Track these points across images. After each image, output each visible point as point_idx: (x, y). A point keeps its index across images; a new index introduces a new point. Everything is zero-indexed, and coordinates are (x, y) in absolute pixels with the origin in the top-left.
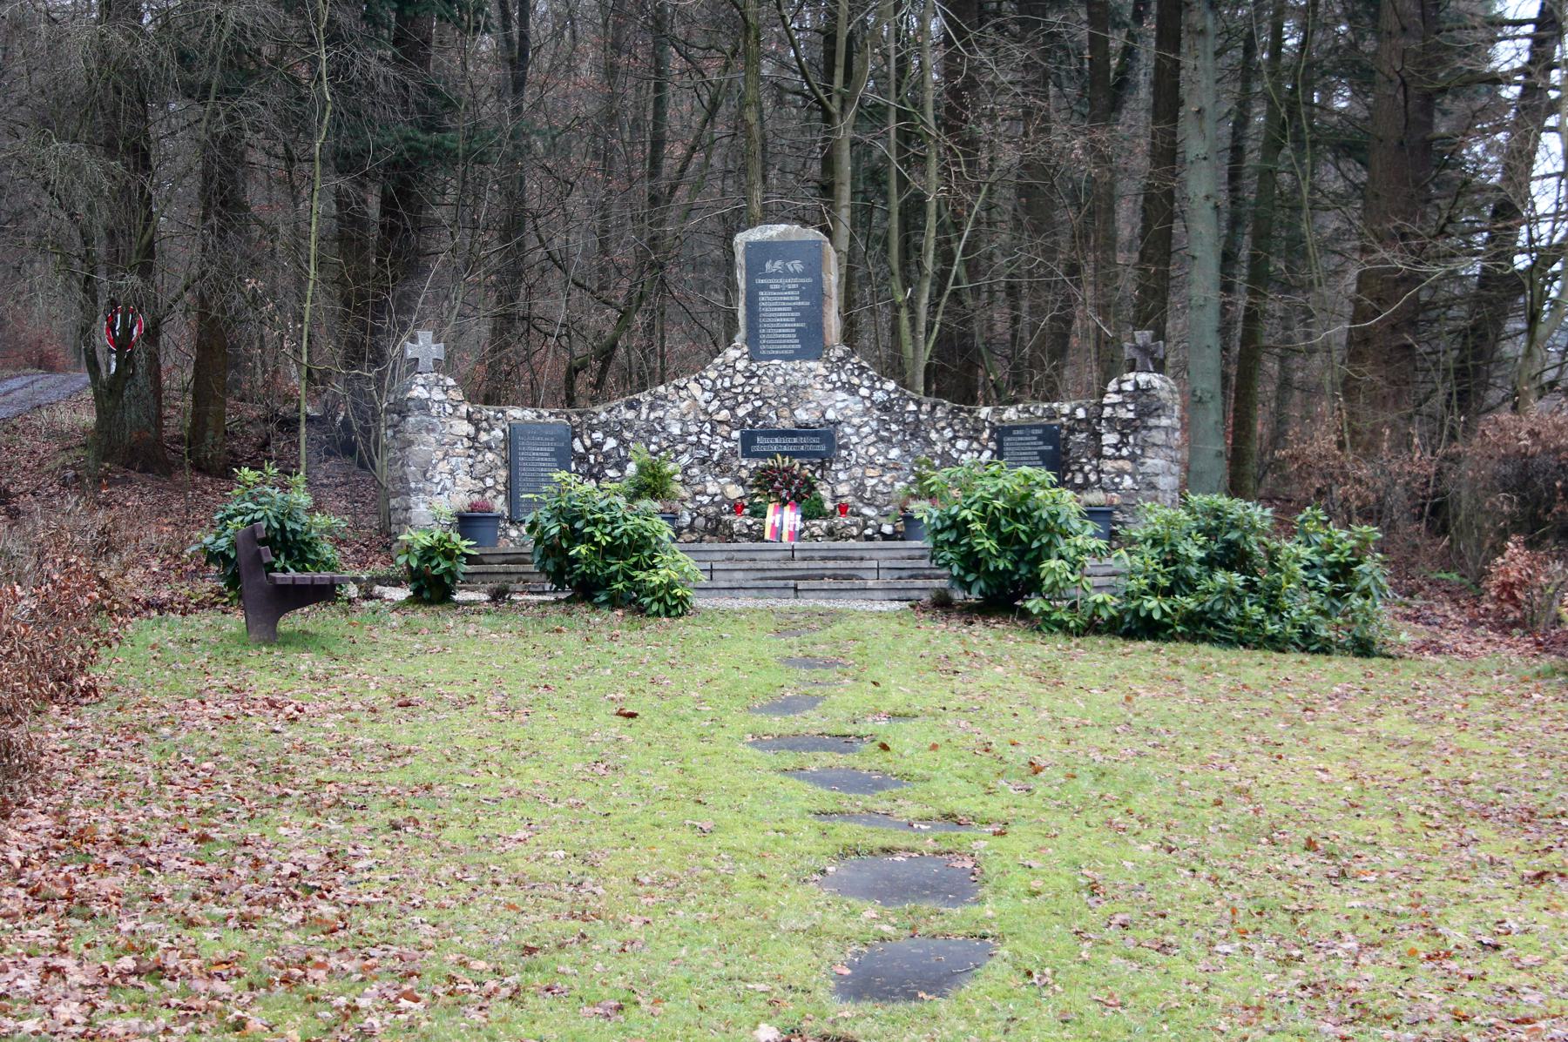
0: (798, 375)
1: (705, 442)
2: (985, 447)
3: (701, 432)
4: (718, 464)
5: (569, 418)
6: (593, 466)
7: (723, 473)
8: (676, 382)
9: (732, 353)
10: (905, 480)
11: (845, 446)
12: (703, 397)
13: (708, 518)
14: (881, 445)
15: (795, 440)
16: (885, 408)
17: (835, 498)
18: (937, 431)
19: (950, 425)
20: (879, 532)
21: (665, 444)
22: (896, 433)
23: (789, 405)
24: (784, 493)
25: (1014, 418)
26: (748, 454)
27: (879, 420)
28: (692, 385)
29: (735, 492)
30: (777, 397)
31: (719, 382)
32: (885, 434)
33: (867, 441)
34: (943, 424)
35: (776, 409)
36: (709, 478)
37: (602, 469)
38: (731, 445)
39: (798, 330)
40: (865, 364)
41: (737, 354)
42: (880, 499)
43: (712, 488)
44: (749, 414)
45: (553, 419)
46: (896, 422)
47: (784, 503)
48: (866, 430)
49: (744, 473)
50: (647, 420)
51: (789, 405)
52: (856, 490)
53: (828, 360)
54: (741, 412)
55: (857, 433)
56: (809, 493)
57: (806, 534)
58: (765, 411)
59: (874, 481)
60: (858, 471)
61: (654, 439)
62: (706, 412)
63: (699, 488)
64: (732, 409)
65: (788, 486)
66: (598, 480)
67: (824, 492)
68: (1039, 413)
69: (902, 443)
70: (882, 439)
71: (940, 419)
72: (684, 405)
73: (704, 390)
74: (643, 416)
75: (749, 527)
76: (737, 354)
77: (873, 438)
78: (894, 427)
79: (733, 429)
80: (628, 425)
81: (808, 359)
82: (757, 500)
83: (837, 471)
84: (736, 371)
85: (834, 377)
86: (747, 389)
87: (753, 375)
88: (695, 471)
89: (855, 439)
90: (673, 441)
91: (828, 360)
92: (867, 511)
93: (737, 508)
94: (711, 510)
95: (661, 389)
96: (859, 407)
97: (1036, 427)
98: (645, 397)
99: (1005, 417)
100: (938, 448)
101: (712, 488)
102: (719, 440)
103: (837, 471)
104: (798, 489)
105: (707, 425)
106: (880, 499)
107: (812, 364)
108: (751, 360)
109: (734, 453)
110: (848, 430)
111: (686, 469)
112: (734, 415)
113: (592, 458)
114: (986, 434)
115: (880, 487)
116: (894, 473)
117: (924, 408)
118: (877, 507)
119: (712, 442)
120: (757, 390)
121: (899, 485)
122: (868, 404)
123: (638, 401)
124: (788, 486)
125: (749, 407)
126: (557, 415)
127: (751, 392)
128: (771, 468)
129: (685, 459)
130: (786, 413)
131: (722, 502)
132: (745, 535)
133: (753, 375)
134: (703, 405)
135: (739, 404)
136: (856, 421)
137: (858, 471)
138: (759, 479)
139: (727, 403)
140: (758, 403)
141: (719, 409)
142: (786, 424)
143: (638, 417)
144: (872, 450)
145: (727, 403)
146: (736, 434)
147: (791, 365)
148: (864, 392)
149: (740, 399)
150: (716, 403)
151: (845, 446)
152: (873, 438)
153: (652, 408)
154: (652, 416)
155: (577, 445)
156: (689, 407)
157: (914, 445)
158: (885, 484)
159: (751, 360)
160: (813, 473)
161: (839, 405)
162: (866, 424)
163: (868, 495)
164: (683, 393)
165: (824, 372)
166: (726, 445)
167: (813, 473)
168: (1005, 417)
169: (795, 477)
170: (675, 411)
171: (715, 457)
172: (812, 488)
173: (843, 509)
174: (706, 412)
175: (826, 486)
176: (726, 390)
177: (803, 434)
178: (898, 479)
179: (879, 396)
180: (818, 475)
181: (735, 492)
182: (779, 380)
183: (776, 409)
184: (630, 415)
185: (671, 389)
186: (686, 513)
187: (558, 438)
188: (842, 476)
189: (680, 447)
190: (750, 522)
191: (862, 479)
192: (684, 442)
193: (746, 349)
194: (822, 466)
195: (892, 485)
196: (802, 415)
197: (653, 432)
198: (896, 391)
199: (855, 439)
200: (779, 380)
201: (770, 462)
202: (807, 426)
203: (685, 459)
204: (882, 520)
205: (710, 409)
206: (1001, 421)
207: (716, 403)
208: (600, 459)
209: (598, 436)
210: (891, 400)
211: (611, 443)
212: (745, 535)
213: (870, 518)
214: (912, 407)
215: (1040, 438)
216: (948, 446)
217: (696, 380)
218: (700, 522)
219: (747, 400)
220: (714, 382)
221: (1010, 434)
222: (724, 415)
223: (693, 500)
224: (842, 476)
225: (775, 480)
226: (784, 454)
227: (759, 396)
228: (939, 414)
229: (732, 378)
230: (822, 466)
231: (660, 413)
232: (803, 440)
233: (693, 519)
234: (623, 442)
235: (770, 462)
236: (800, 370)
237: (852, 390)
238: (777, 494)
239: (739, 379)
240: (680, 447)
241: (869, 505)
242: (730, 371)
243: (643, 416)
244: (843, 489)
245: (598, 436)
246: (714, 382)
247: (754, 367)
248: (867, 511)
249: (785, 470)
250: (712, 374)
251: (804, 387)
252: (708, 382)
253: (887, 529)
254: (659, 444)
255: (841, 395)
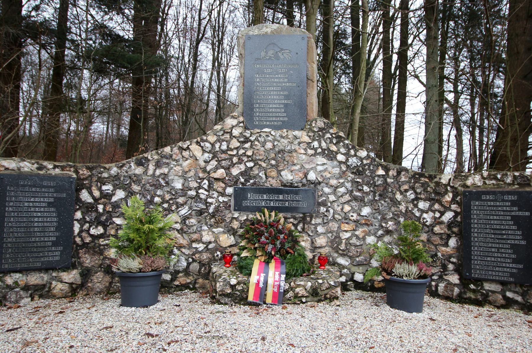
0: (285, 141)
1: (203, 197)
2: (449, 209)
3: (200, 187)
4: (213, 216)
5: (77, 172)
6: (102, 215)
7: (217, 224)
8: (180, 144)
9: (230, 122)
10: (375, 234)
11: (324, 204)
12: (202, 157)
13: (202, 264)
14: (354, 204)
15: (281, 197)
16: (358, 171)
17: (314, 248)
18: (401, 193)
19: (413, 188)
20: (352, 279)
21: (168, 197)
22: (367, 194)
23: (276, 166)
24: (269, 248)
25: (480, 184)
26: (239, 208)
27: (353, 182)
28: (194, 147)
29: (227, 240)
30: (267, 160)
31: (217, 146)
32: (358, 194)
33: (343, 200)
34: (406, 187)
35: (265, 170)
36: (205, 228)
37: (111, 217)
38: (226, 199)
39: (286, 105)
40: (342, 134)
41: (234, 122)
42: (353, 251)
43: (207, 237)
44: (242, 174)
45: (58, 171)
46: (368, 184)
47: (269, 257)
48: (342, 190)
49: (236, 225)
50: (153, 175)
51: (276, 166)
52: (332, 242)
53: (311, 130)
54: (235, 171)
55: (334, 192)
56: (293, 247)
57: (290, 294)
58: (256, 171)
59: (348, 235)
60: (334, 226)
61: (159, 192)
62: (204, 170)
63: (195, 236)
64: (227, 169)
65: (273, 239)
66: (105, 227)
67: (305, 243)
68: (509, 180)
69: (372, 203)
70: (355, 199)
71: (404, 183)
72: (186, 164)
73: (204, 151)
74: (150, 172)
75: (233, 287)
76: (234, 122)
77: (347, 197)
78: (366, 188)
79: (227, 185)
80: (137, 179)
81: (294, 130)
82: (244, 254)
83: (316, 225)
84: (232, 137)
85: (316, 144)
86: (241, 152)
87: (247, 140)
88: (193, 221)
89: (332, 198)
90: (175, 194)
91: (311, 130)
92: (342, 261)
93: (227, 259)
94: (205, 256)
95: (167, 149)
96: (337, 171)
97: (509, 193)
98: (152, 156)
99: (469, 182)
100: (403, 208)
101: (207, 237)
102: (216, 195)
103: (316, 225)
104: (283, 244)
105: (206, 181)
106: (353, 251)
107: (297, 133)
108: (246, 128)
109: (227, 206)
110: (327, 190)
111: (185, 219)
112: (229, 174)
113: (100, 208)
114: (449, 197)
115: (354, 241)
116: (366, 228)
117: (391, 173)
118: (350, 257)
119: (209, 196)
120: (249, 153)
121: (371, 240)
122: (344, 168)
123: (147, 159)
124: (273, 239)
125: (242, 167)
126: (63, 168)
127: (244, 154)
128: (259, 222)
129: (184, 211)
130: (274, 173)
131: (216, 249)
132: (228, 295)
133: (247, 140)
134: (203, 164)
135: (233, 165)
136: (334, 182)
137: (334, 226)
138: (247, 232)
139: (224, 163)
140: (251, 164)
141: (216, 168)
142: (274, 183)
143: (145, 173)
144: (347, 208)
145: (224, 163)
146: (230, 190)
147: (279, 133)
148: (341, 158)
149: (235, 160)
150: (214, 163)
151: (324, 204)
152: (347, 197)
153: (158, 165)
154: (158, 172)
155: (85, 195)
156: (190, 166)
157: (383, 205)
158: (357, 237)
159: (246, 128)
160: (295, 226)
161: (320, 168)
162: (342, 185)
163: (343, 247)
164: (186, 154)
165: (307, 139)
166: (221, 199)
167: (295, 226)
168: (469, 182)
169: (280, 232)
170: (178, 168)
171: (211, 210)
172: (295, 242)
173: (324, 261)
174: (204, 170)
175: (306, 237)
176: (224, 152)
177: (287, 192)
178: (368, 234)
179: (353, 161)
180: (299, 228)
181: (227, 240)
182: (269, 145)
183: (265, 170)
184: (139, 171)
185: (176, 150)
186: (183, 259)
187: (59, 189)
188: (320, 229)
189: (181, 200)
190: (233, 281)
191: (338, 233)
192: (185, 195)
193: (241, 119)
194: (303, 220)
195: (364, 239)
196: (287, 176)
197: (158, 186)
198: (368, 157)
199: (332, 198)
200: (269, 145)
201: (258, 216)
202: (291, 185)
203: (184, 211)
204: (354, 269)
205: (208, 168)
206: (465, 186)
207: (214, 163)
208: (109, 208)
209: (108, 188)
210: (363, 165)
211: (120, 194)
212: (228, 295)
213: (344, 267)
214: (381, 172)
215: (513, 203)
216: (411, 206)
217: (198, 143)
218: (195, 267)
219: (240, 161)
220: (213, 145)
221: (479, 199)
222: (221, 173)
223: (190, 247)
224: (320, 229)
225: (260, 234)
226: (271, 209)
227: (251, 158)
228: (403, 179)
229: (228, 142)
230: (303, 220)
231: (165, 170)
232: (289, 197)
233: (189, 264)
234: (131, 193)
235: (258, 216)
236: (287, 137)
237: (331, 156)
238: (263, 249)
239: (235, 143)
240: (181, 200)
241: (343, 255)
242: (228, 136)
243: (150, 172)
244: (321, 241)
245: (108, 188)
246: (213, 145)
247: (247, 134)
248: (342, 261)
249: (271, 225)
250: (212, 138)
251: (290, 152)
252: (208, 145)
253: (359, 277)
254: (162, 197)
255: (321, 160)
